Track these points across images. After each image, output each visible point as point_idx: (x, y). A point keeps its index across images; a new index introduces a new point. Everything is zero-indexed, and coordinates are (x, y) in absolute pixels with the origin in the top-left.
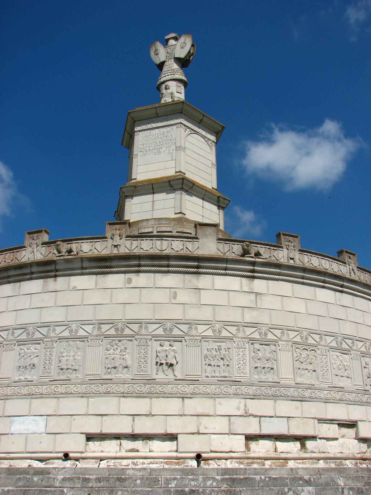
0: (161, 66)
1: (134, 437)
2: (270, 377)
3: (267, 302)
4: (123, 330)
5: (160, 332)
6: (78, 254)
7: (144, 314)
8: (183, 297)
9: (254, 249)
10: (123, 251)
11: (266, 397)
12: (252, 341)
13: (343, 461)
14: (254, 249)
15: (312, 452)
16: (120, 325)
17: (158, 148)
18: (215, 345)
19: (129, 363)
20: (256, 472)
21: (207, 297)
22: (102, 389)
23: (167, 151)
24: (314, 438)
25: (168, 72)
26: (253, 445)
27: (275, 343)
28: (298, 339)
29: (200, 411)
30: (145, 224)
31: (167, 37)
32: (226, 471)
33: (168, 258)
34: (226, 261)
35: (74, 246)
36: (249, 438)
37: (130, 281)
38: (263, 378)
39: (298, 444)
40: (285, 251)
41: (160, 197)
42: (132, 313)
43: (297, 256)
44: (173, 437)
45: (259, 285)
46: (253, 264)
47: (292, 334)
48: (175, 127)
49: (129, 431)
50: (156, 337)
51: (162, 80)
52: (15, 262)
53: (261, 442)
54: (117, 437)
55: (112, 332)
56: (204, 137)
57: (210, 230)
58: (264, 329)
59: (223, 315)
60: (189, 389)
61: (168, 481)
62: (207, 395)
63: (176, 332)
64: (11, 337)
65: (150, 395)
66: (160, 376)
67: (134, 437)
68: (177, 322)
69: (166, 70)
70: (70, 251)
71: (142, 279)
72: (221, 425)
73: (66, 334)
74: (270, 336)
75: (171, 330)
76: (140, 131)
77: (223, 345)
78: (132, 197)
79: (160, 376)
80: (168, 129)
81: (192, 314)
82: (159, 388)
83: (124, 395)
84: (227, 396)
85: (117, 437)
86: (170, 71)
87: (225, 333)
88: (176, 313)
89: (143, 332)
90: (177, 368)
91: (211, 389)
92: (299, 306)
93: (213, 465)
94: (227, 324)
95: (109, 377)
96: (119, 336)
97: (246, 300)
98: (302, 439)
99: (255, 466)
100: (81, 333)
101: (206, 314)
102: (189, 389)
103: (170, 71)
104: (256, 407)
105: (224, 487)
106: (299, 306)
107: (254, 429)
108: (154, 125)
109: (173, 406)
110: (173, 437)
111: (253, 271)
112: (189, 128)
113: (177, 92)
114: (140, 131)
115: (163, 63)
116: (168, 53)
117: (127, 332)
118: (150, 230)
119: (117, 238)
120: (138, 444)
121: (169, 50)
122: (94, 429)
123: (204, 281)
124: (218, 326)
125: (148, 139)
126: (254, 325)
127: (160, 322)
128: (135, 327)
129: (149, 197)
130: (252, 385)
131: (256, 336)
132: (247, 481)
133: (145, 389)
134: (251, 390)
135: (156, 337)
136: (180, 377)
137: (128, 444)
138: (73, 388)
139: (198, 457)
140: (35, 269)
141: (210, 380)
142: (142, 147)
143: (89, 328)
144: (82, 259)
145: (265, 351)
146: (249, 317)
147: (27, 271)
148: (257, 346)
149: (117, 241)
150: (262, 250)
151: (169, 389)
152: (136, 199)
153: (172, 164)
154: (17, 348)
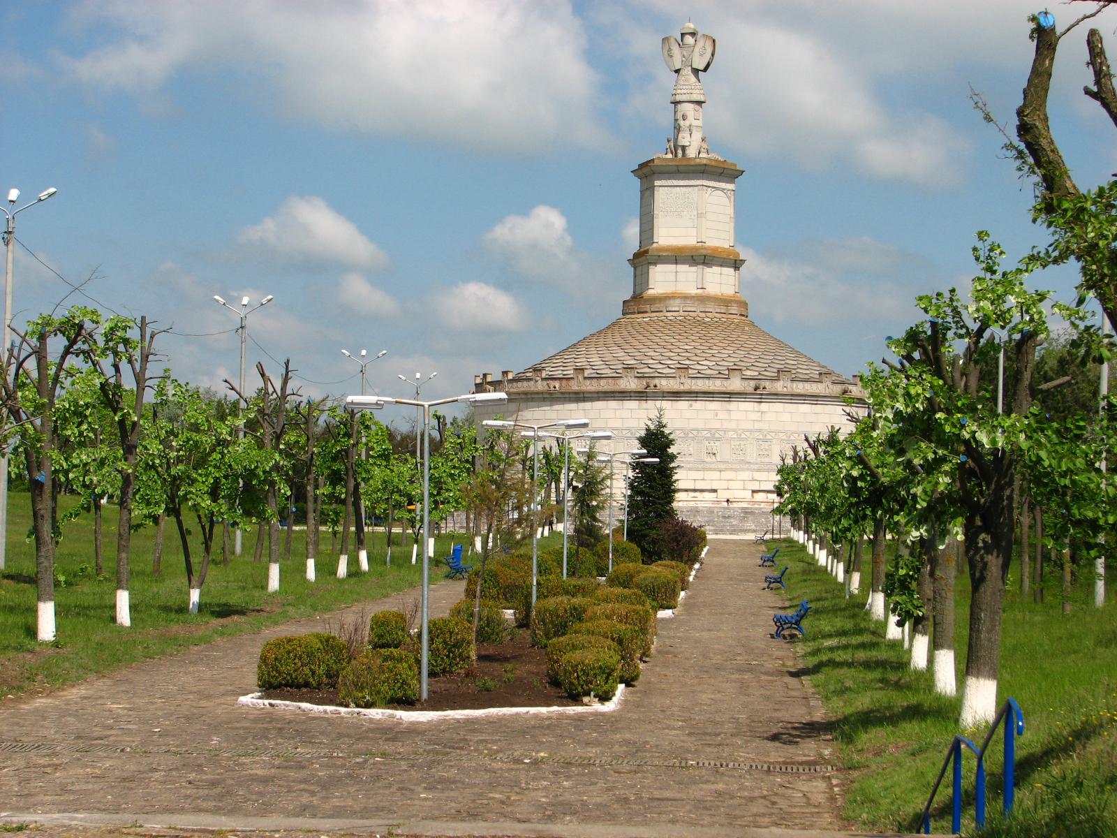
1: (695, 491)
2: (767, 460)
3: (768, 417)
4: (688, 434)
5: (709, 435)
7: (700, 425)
8: (722, 415)
9: (763, 383)
10: (686, 387)
11: (764, 471)
12: (758, 440)
14: (763, 383)
18: (738, 443)
19: (692, 452)
20: (757, 509)
21: (734, 415)
26: (755, 495)
27: (770, 440)
28: (785, 437)
29: (729, 478)
30: (672, 302)
32: (743, 508)
33: (713, 393)
34: (746, 394)
35: (656, 381)
36: (754, 492)
37: (691, 405)
38: (763, 460)
40: (782, 382)
41: (683, 268)
42: (693, 425)
43: (789, 384)
44: (715, 491)
45: (764, 406)
46: (761, 394)
47: (781, 435)
48: (696, 188)
49: (693, 488)
50: (707, 439)
51: (678, 98)
52: (617, 388)
53: (760, 494)
54: (686, 490)
56: (723, 190)
57: (737, 373)
59: (743, 426)
60: (723, 466)
61: (718, 512)
62: (731, 469)
63: (717, 435)
64: (620, 434)
65: (704, 470)
66: (709, 460)
67: (695, 491)
68: (718, 430)
70: (655, 386)
71: (698, 405)
72: (739, 485)
74: (768, 437)
76: (660, 186)
78: (655, 264)
80: (690, 189)
81: (727, 425)
82: (708, 466)
83: (690, 469)
84: (743, 470)
85: (686, 490)
87: (743, 436)
88: (716, 425)
89: (700, 435)
90: (718, 455)
91: (735, 466)
92: (786, 417)
93: (735, 505)
94: (744, 431)
97: (756, 416)
99: (756, 506)
101: (733, 425)
102: (723, 466)
104: (758, 475)
105: (742, 515)
106: (786, 417)
108: (676, 182)
109: (716, 475)
110: (715, 491)
111: (761, 398)
112: (709, 187)
114: (660, 186)
115: (680, 70)
116: (684, 56)
117: (690, 435)
118: (677, 309)
119: (683, 378)
120: (697, 494)
121: (685, 53)
123: (733, 405)
126: (759, 430)
127: (709, 430)
128: (695, 433)
129: (672, 267)
130: (757, 464)
131: (761, 437)
132: (752, 513)
134: (756, 467)
135: (707, 439)
137: (692, 494)
139: (728, 501)
140: (632, 395)
144: (663, 392)
145: (765, 445)
146: (757, 426)
147: (628, 395)
148: (761, 443)
149: (683, 380)
150: (767, 384)
151: (713, 466)
152: (660, 268)
153: (693, 232)
154: (626, 442)
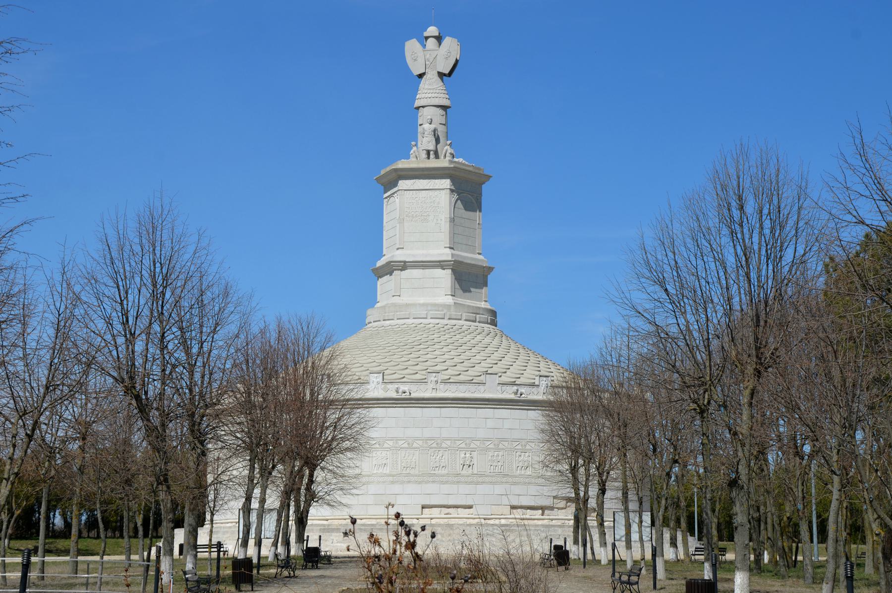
0: (421, 76)
5: (463, 445)
6: (410, 393)
13: (566, 521)
15: (548, 516)
16: (439, 441)
17: (425, 214)
22: (431, 479)
23: (435, 220)
24: (551, 508)
25: (429, 91)
31: (426, 34)
39: (540, 511)
44: (470, 507)
55: (434, 445)
58: (523, 443)
60: (480, 479)
69: (426, 87)
73: (406, 445)
75: (470, 444)
77: (501, 453)
79: (464, 472)
80: (438, 192)
82: (463, 479)
86: (431, 91)
95: (433, 472)
96: (439, 447)
98: (543, 509)
100: (415, 445)
103: (431, 91)
104: (517, 489)
107: (515, 503)
110: (470, 507)
113: (440, 124)
117: (444, 445)
122: (427, 503)
124: (496, 442)
125: (414, 201)
133: (456, 479)
136: (475, 472)
138: (412, 479)
141: (492, 474)
142: (408, 211)
143: (420, 442)
